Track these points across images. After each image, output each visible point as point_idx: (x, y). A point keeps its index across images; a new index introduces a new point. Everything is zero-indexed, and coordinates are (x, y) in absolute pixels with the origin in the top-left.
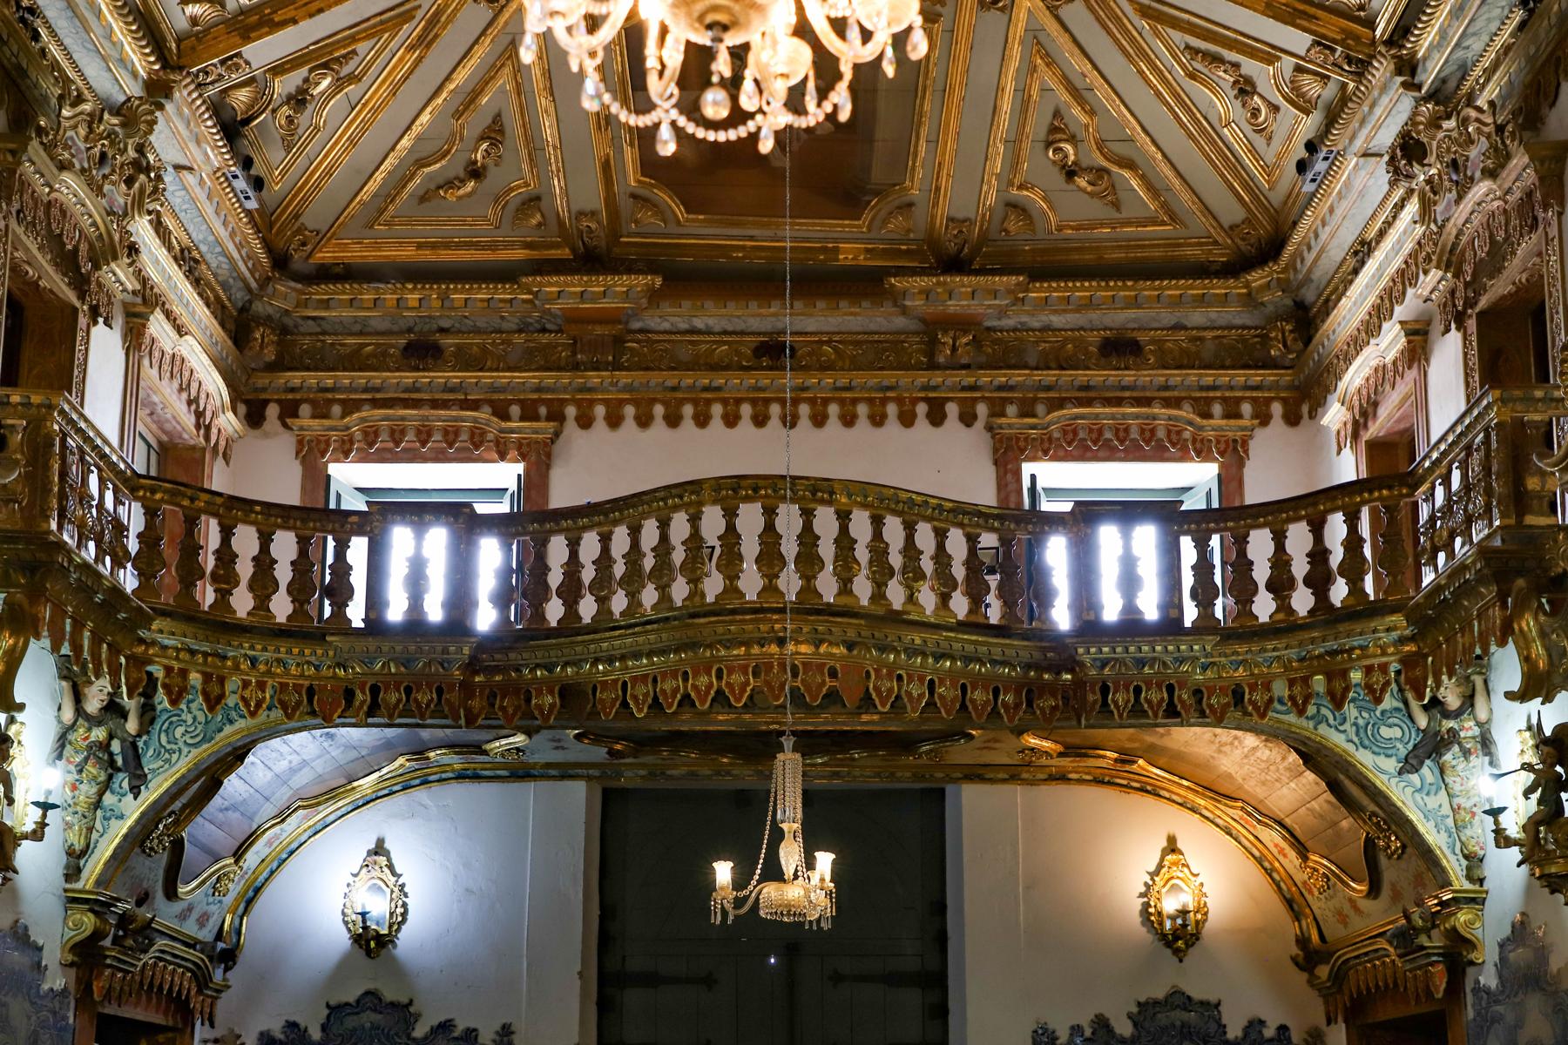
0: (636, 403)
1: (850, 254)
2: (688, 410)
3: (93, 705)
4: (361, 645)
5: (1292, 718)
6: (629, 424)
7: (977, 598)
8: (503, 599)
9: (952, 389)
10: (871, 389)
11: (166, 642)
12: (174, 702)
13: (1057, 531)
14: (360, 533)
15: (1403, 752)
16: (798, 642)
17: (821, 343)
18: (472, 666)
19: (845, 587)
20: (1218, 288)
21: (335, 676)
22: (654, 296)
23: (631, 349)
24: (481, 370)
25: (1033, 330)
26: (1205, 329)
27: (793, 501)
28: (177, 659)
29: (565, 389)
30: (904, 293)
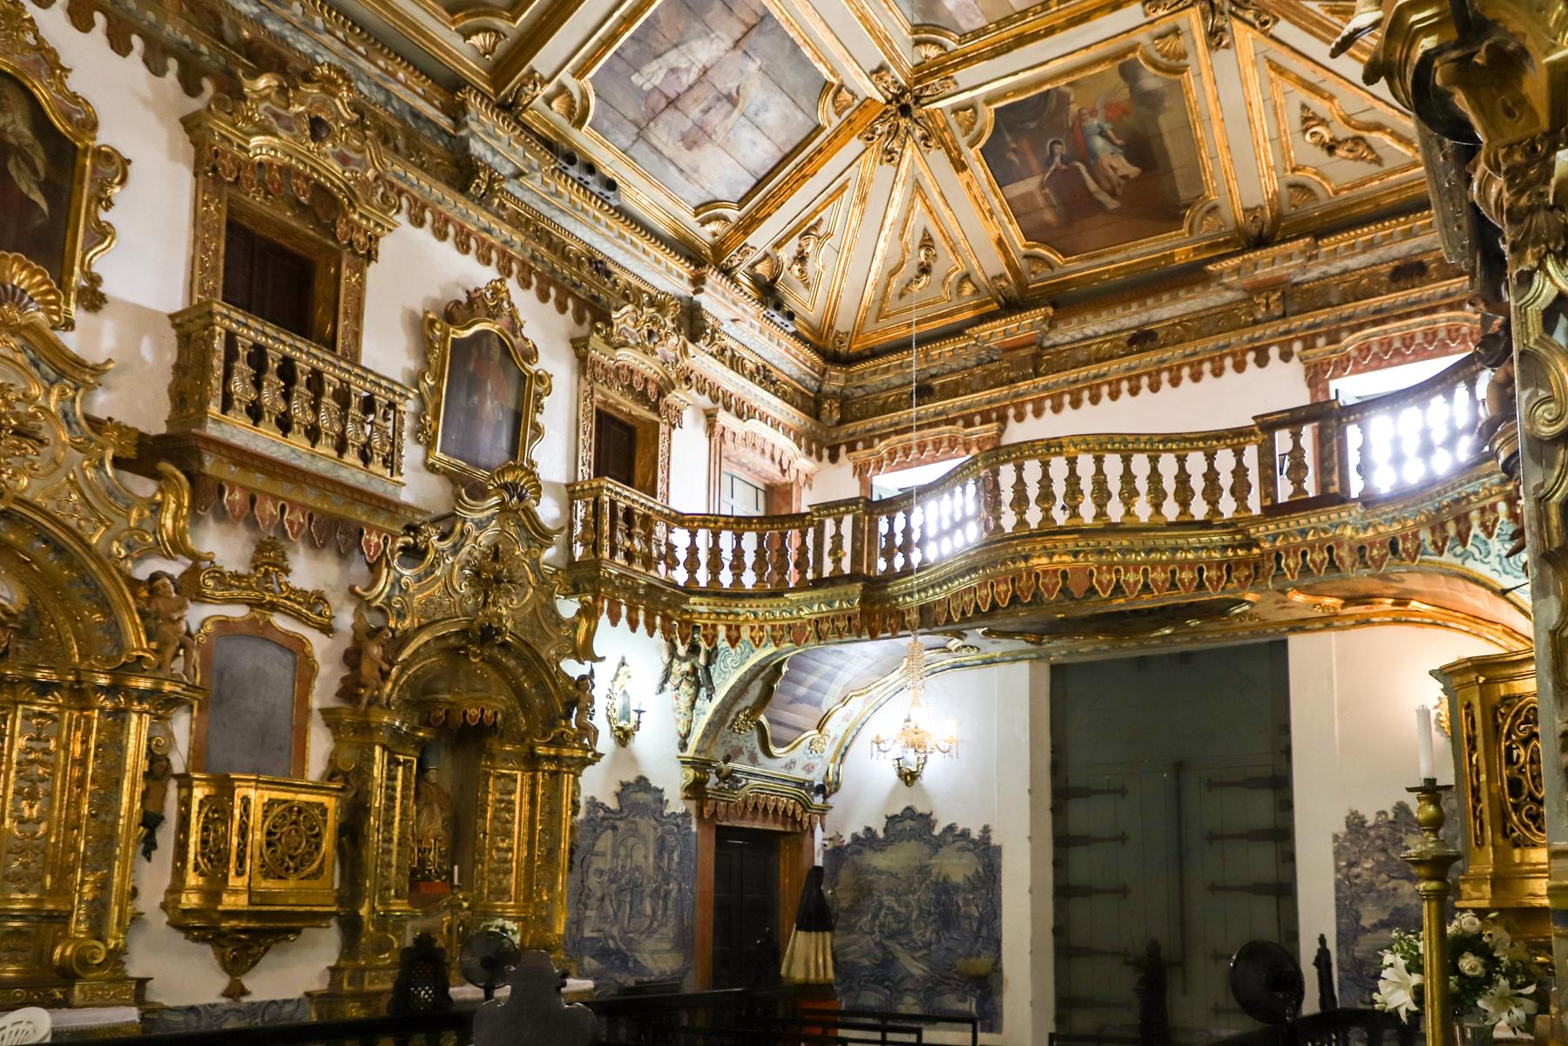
1: (1182, 256)
17: (1174, 324)
24: (956, 396)
25: (1333, 276)
29: (1006, 397)
30: (1221, 274)
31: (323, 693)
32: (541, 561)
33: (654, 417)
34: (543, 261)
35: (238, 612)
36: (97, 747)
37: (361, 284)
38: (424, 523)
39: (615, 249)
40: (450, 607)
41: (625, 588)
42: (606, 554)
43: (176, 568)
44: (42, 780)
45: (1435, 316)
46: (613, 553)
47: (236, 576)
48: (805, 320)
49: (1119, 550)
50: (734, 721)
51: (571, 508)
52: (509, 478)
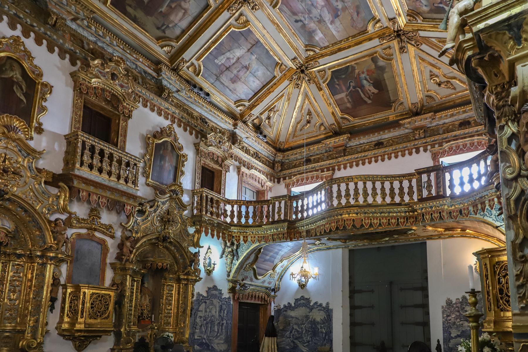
1: (392, 118)
10: (401, 148)
17: (389, 140)
25: (440, 125)
29: (335, 163)
30: (404, 124)
31: (111, 258)
32: (183, 215)
33: (220, 169)
34: (185, 119)
35: (84, 231)
36: (36, 275)
37: (126, 126)
38: (145, 202)
39: (208, 115)
40: (153, 230)
41: (210, 224)
42: (204, 213)
43: (64, 217)
44: (18, 286)
45: (473, 138)
46: (206, 213)
47: (83, 219)
48: (270, 138)
49: (371, 213)
50: (245, 267)
51: (193, 198)
52: (173, 188)
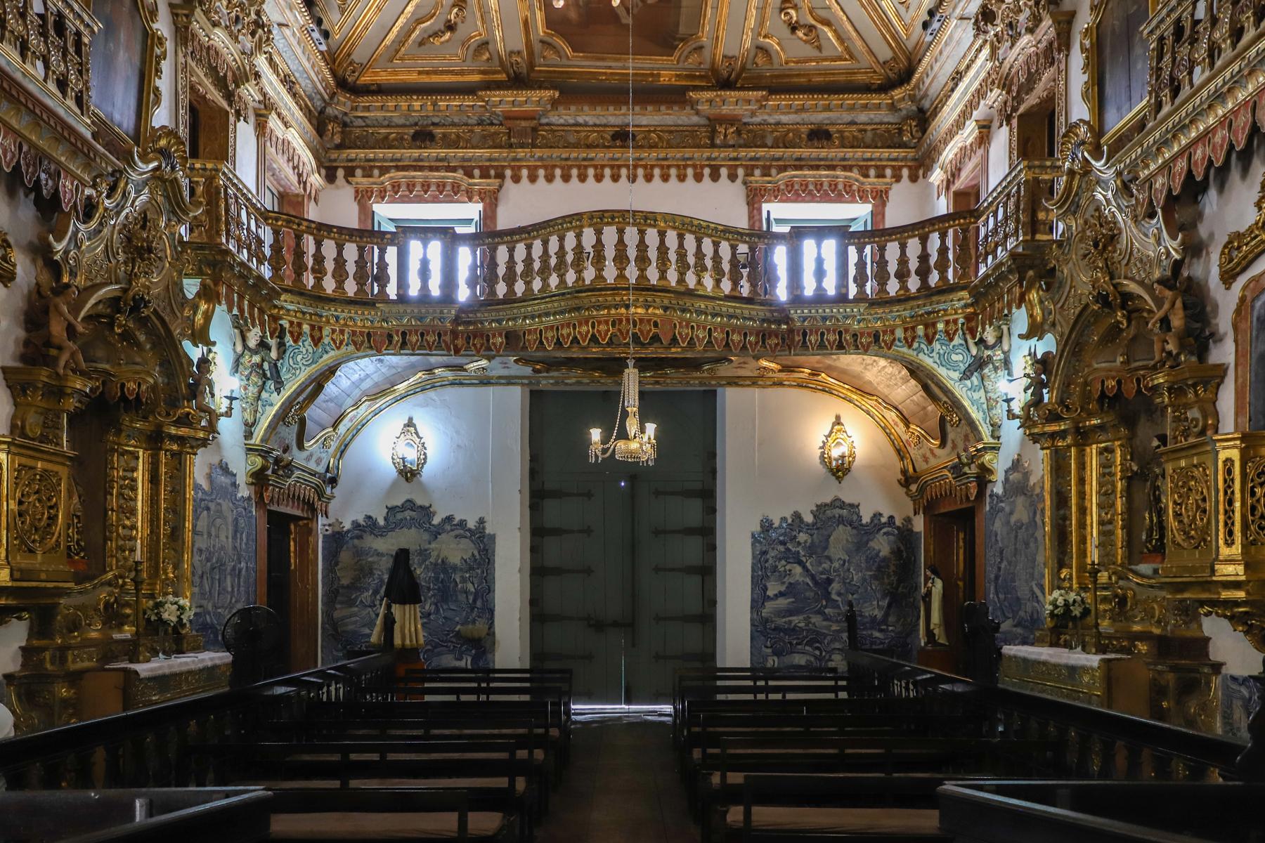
0: (545, 167)
1: (667, 78)
2: (575, 172)
3: (252, 343)
4: (395, 309)
5: (905, 350)
6: (541, 180)
7: (735, 282)
8: (472, 283)
9: (724, 159)
10: (678, 159)
11: (289, 307)
12: (296, 341)
13: (781, 244)
14: (392, 244)
15: (963, 367)
16: (636, 307)
18: (457, 321)
19: (663, 276)
20: (875, 99)
21: (382, 327)
22: (555, 103)
23: (543, 136)
24: (457, 148)
26: (868, 124)
27: (634, 225)
28: (295, 316)
29: (505, 159)
